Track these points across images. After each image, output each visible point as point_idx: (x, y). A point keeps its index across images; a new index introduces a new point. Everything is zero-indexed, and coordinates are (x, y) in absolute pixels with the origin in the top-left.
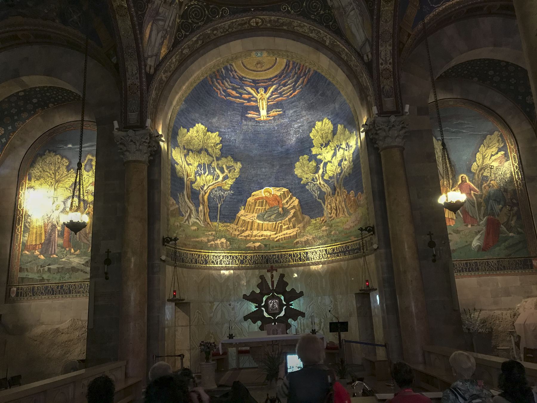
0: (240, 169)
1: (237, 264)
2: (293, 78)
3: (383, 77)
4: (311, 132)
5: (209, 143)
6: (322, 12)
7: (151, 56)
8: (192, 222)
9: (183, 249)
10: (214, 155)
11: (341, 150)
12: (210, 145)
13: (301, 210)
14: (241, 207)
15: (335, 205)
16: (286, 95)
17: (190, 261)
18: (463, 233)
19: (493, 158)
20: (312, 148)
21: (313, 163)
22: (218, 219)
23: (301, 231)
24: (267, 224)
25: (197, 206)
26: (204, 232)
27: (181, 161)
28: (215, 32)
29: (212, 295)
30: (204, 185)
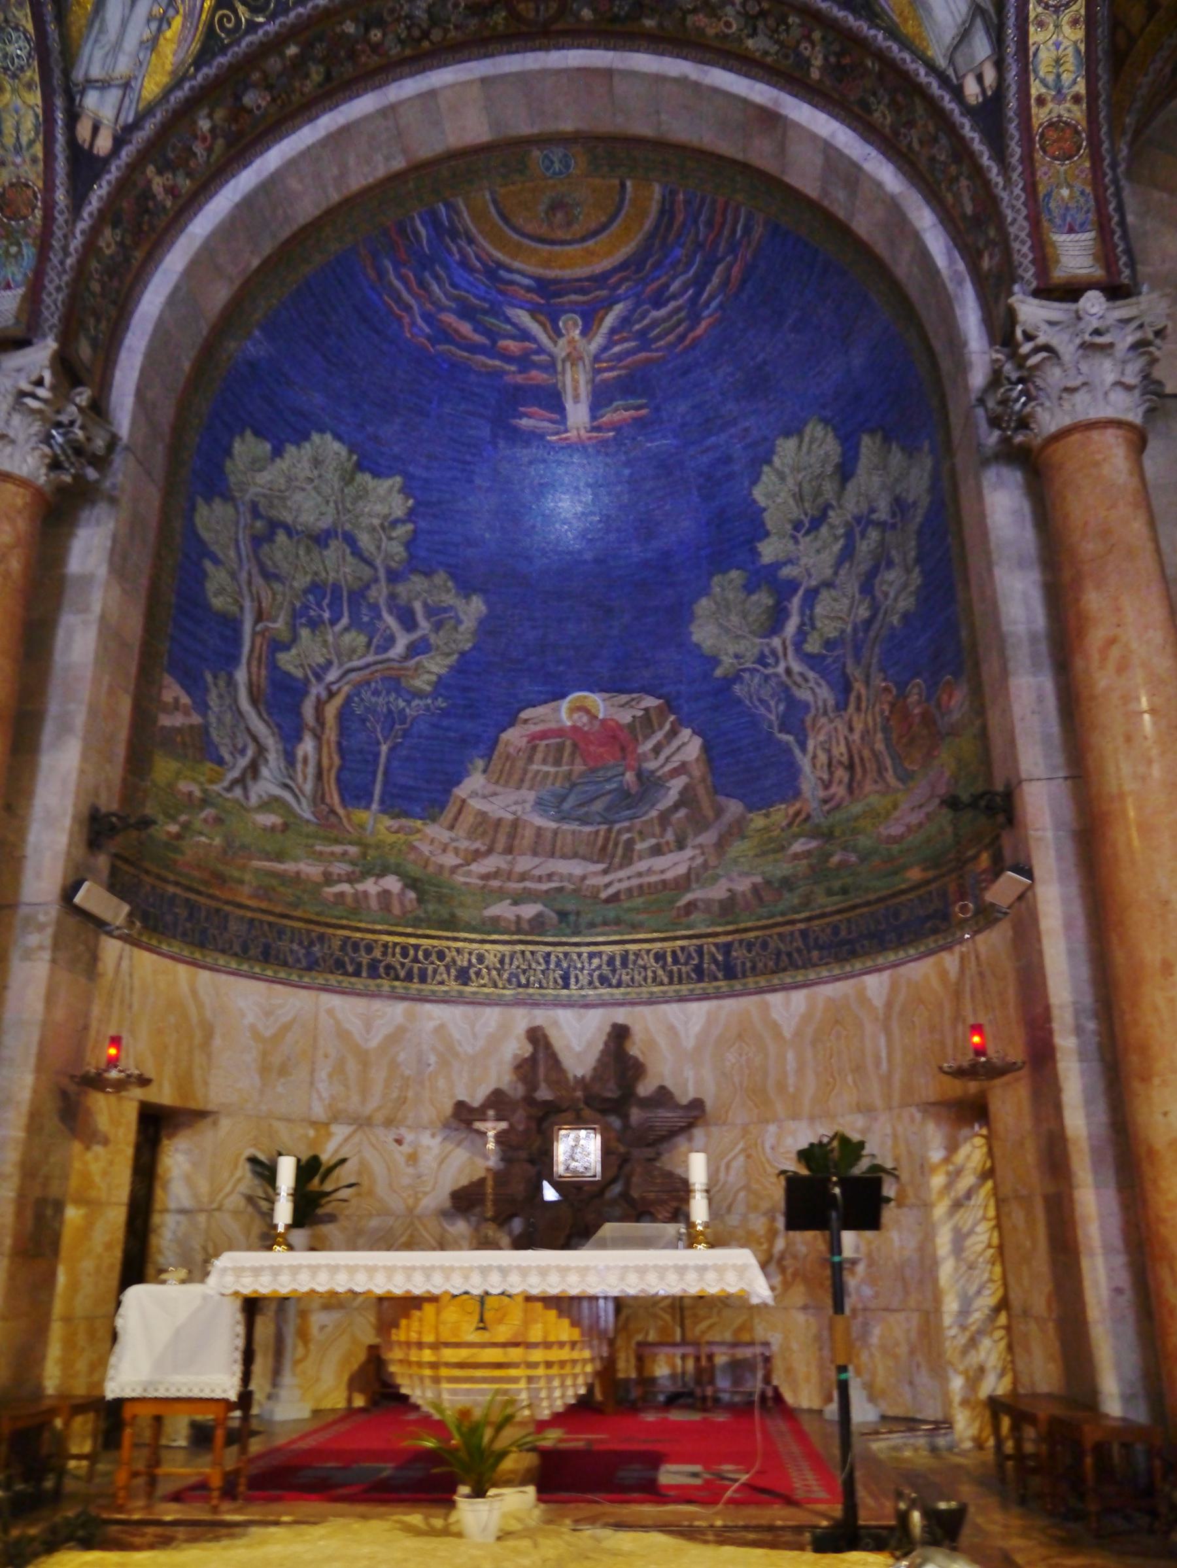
0: (482, 622)
1: (442, 983)
2: (689, 265)
3: (1045, 152)
4: (755, 480)
5: (362, 514)
8: (260, 797)
9: (211, 891)
10: (378, 562)
11: (874, 534)
12: (365, 521)
13: (709, 779)
14: (471, 762)
15: (843, 749)
16: (662, 343)
17: (237, 948)
20: (760, 540)
21: (764, 599)
22: (377, 797)
23: (706, 861)
24: (574, 832)
25: (290, 737)
26: (310, 841)
27: (232, 553)
28: (376, 35)
29: (325, 1095)
30: (329, 663)
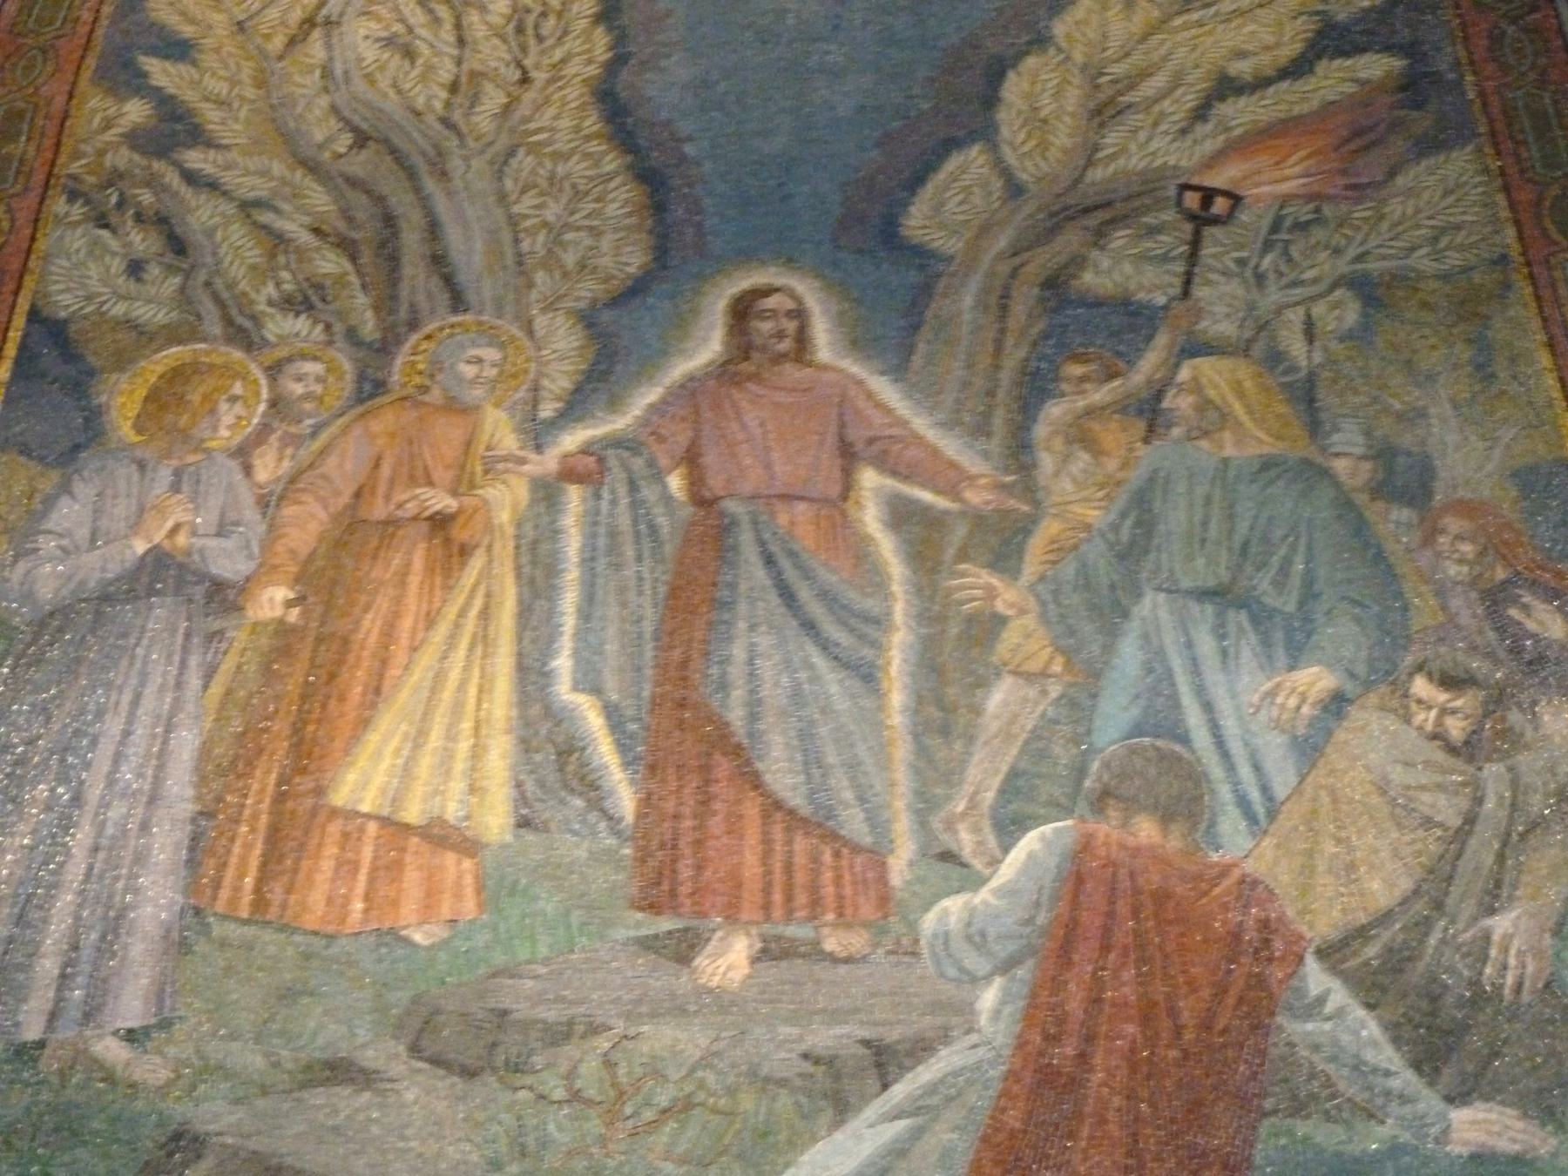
18: (590, 1068)
19: (1242, 113)
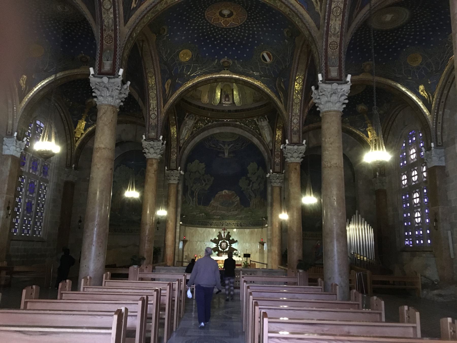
4: (248, 166)
6: (254, 126)
7: (182, 139)
21: (248, 181)
25: (193, 198)
